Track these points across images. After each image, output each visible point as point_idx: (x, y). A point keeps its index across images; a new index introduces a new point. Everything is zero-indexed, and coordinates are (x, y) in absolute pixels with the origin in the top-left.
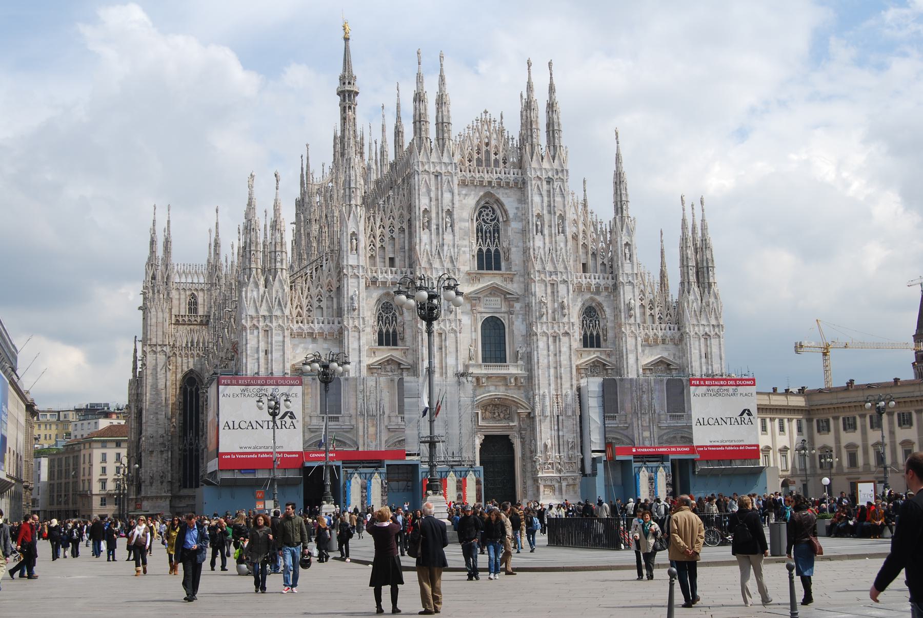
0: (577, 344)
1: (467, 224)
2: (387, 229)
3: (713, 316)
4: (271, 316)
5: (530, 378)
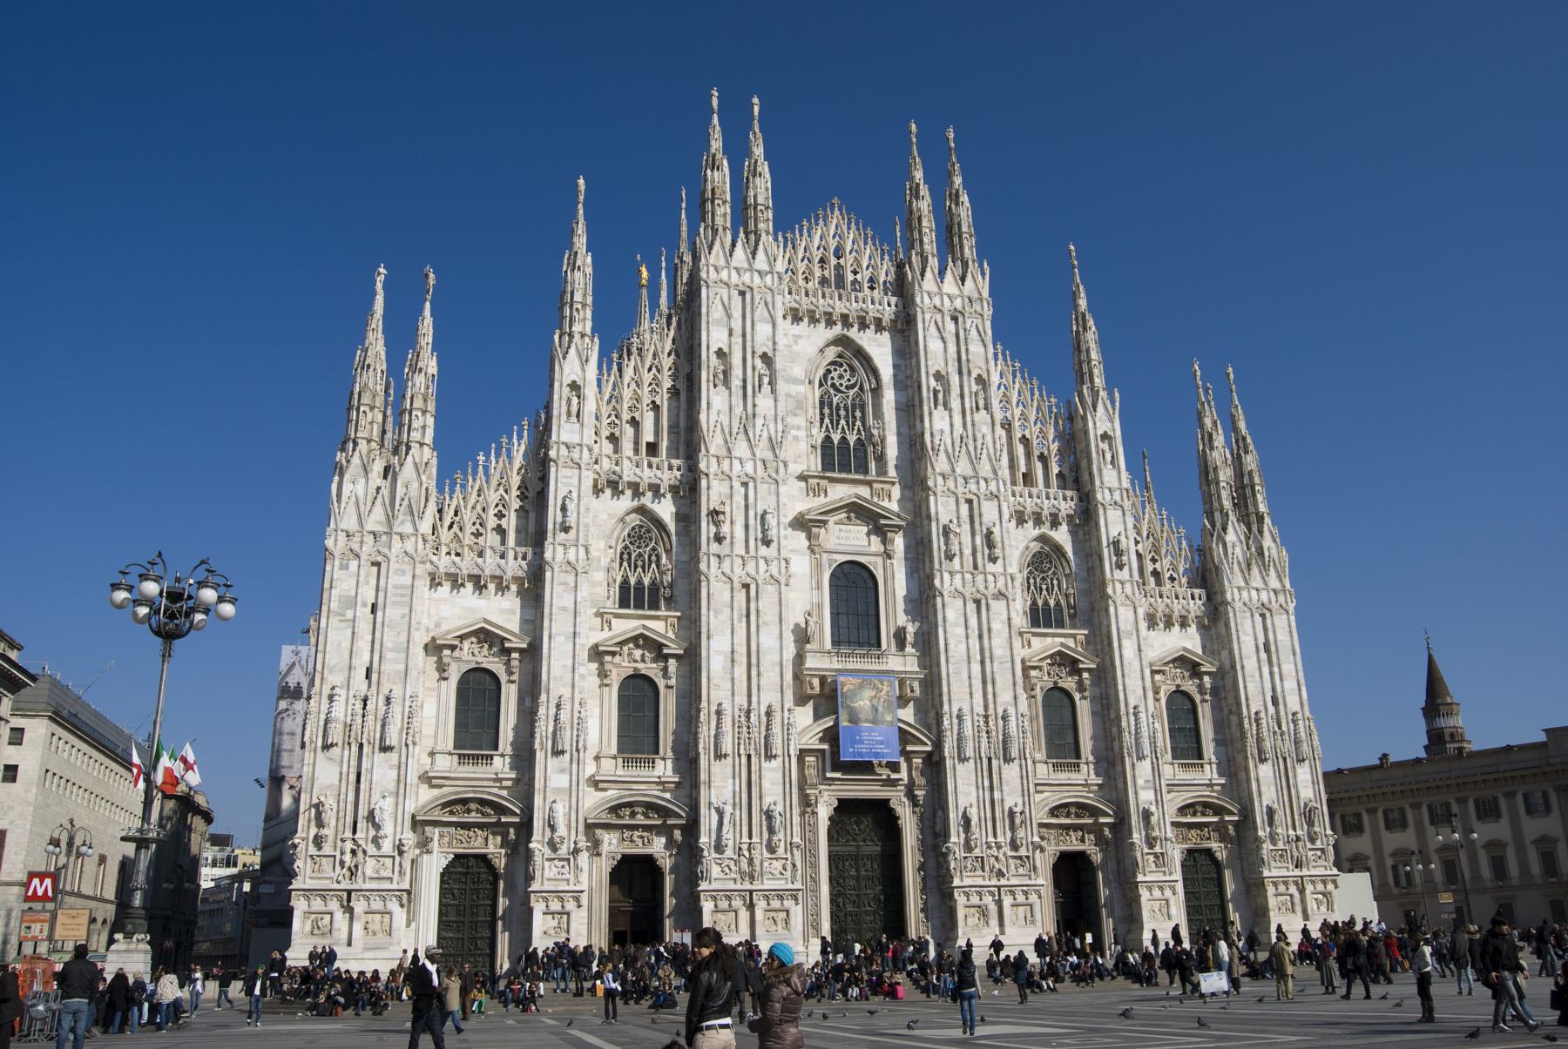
0: (1021, 621)
1: (802, 389)
2: (646, 389)
3: (1272, 572)
4: (389, 534)
5: (932, 682)
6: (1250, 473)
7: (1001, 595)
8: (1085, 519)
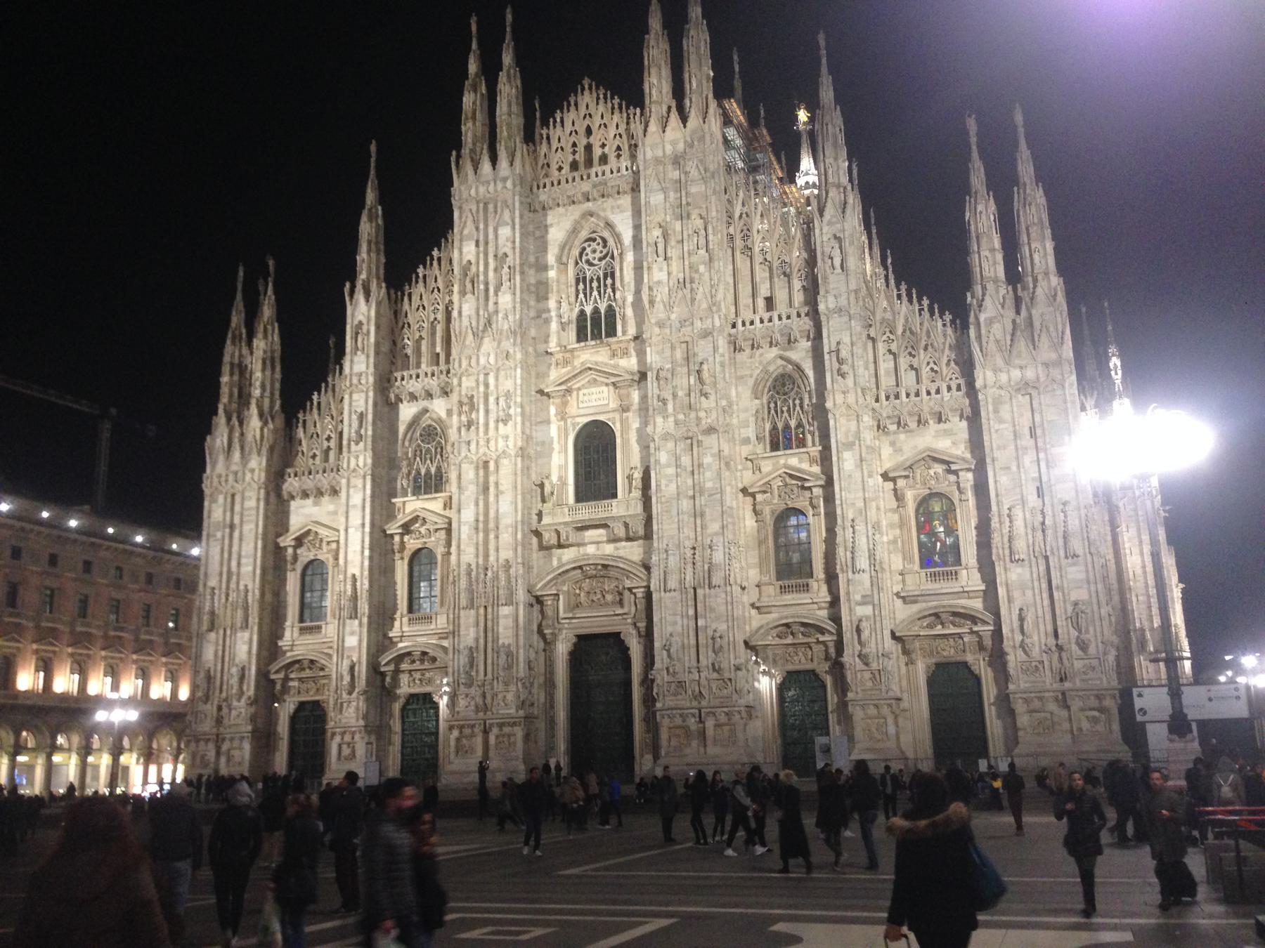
6: (1027, 229)
7: (711, 430)
8: (818, 336)
